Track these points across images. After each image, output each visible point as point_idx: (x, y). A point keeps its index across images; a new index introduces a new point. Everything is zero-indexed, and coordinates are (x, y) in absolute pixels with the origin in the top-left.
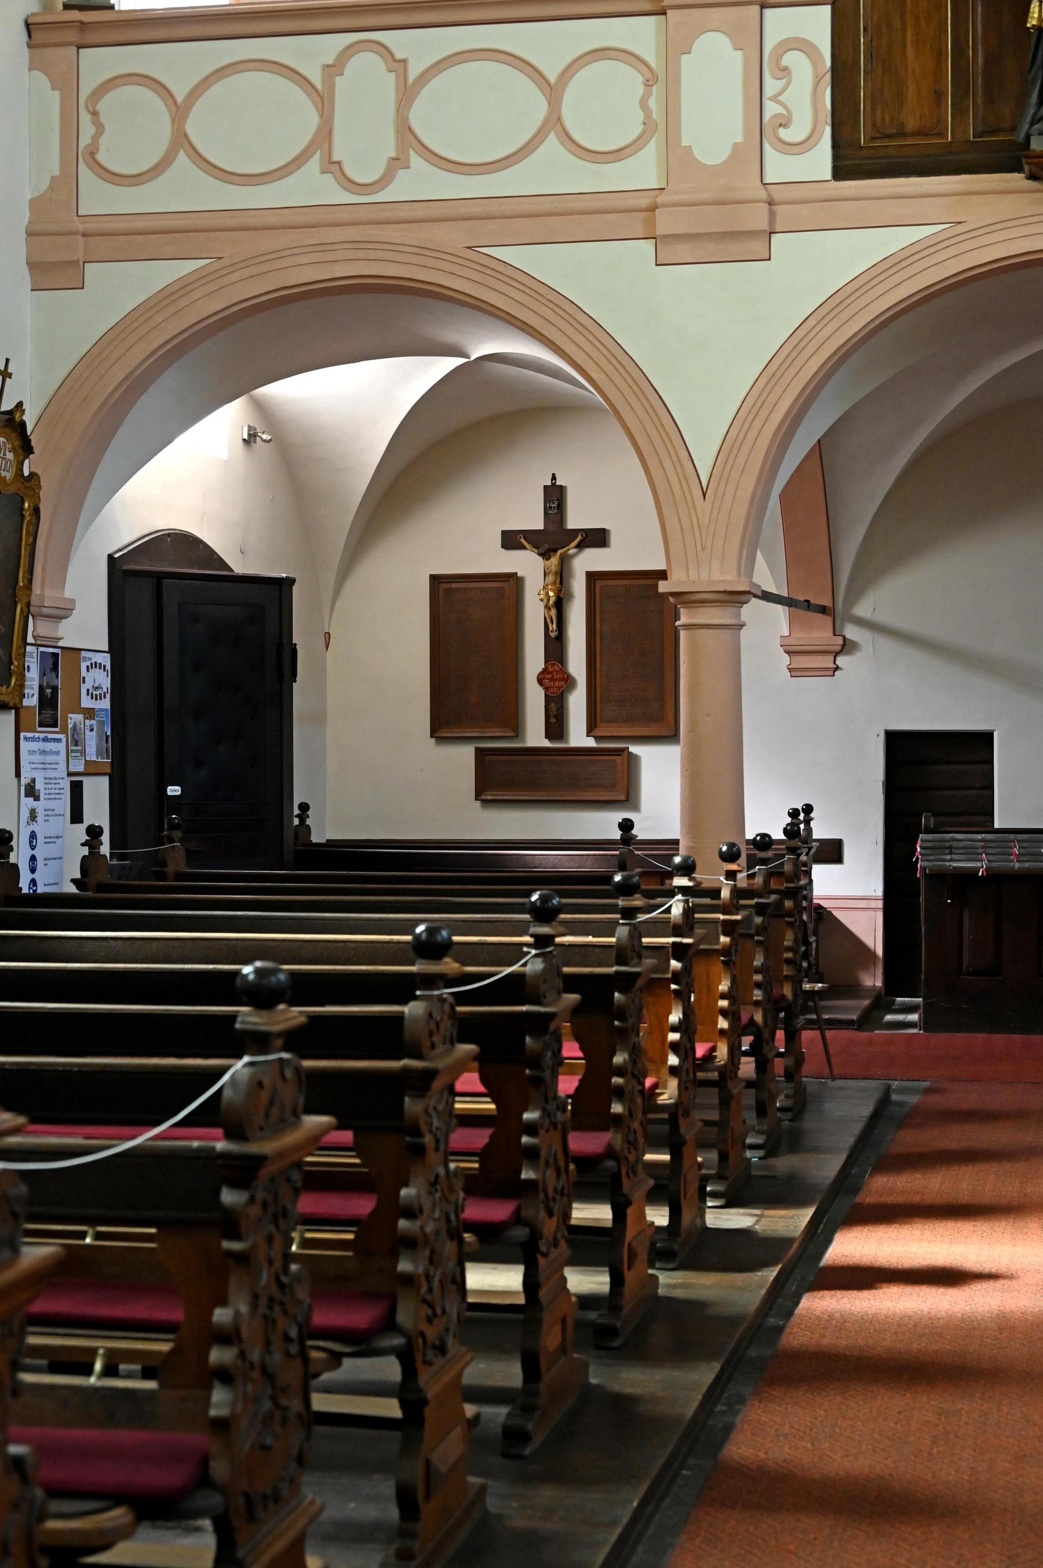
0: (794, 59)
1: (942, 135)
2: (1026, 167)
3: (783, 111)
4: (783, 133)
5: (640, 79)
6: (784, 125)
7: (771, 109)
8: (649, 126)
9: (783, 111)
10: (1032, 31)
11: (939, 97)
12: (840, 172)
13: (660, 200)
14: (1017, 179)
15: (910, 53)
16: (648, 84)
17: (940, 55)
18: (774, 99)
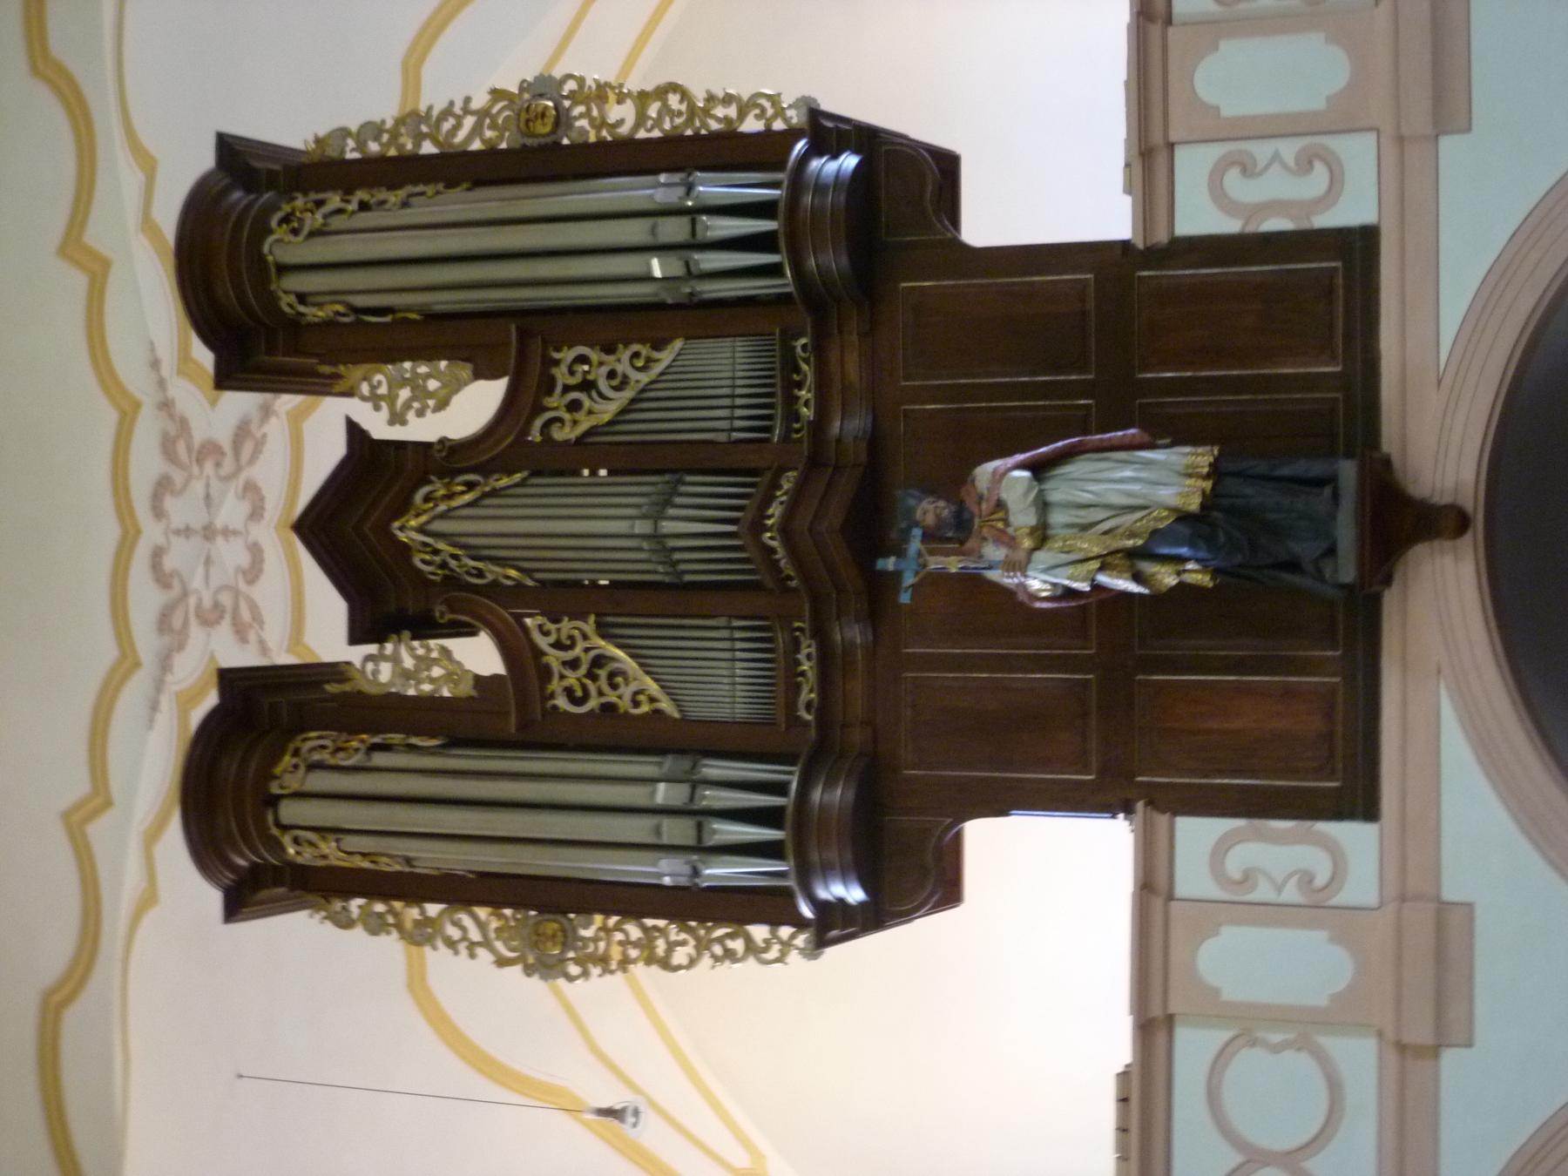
0: (1235, 863)
1: (1333, 690)
2: (1375, 588)
3: (1296, 878)
4: (1320, 880)
5: (1245, 1052)
6: (1311, 881)
7: (1291, 894)
8: (1303, 1044)
9: (1296, 878)
10: (1218, 581)
11: (1288, 693)
12: (1369, 811)
13: (1390, 1035)
14: (1390, 600)
15: (1237, 724)
16: (1253, 1043)
17: (1238, 688)
18: (1279, 889)
